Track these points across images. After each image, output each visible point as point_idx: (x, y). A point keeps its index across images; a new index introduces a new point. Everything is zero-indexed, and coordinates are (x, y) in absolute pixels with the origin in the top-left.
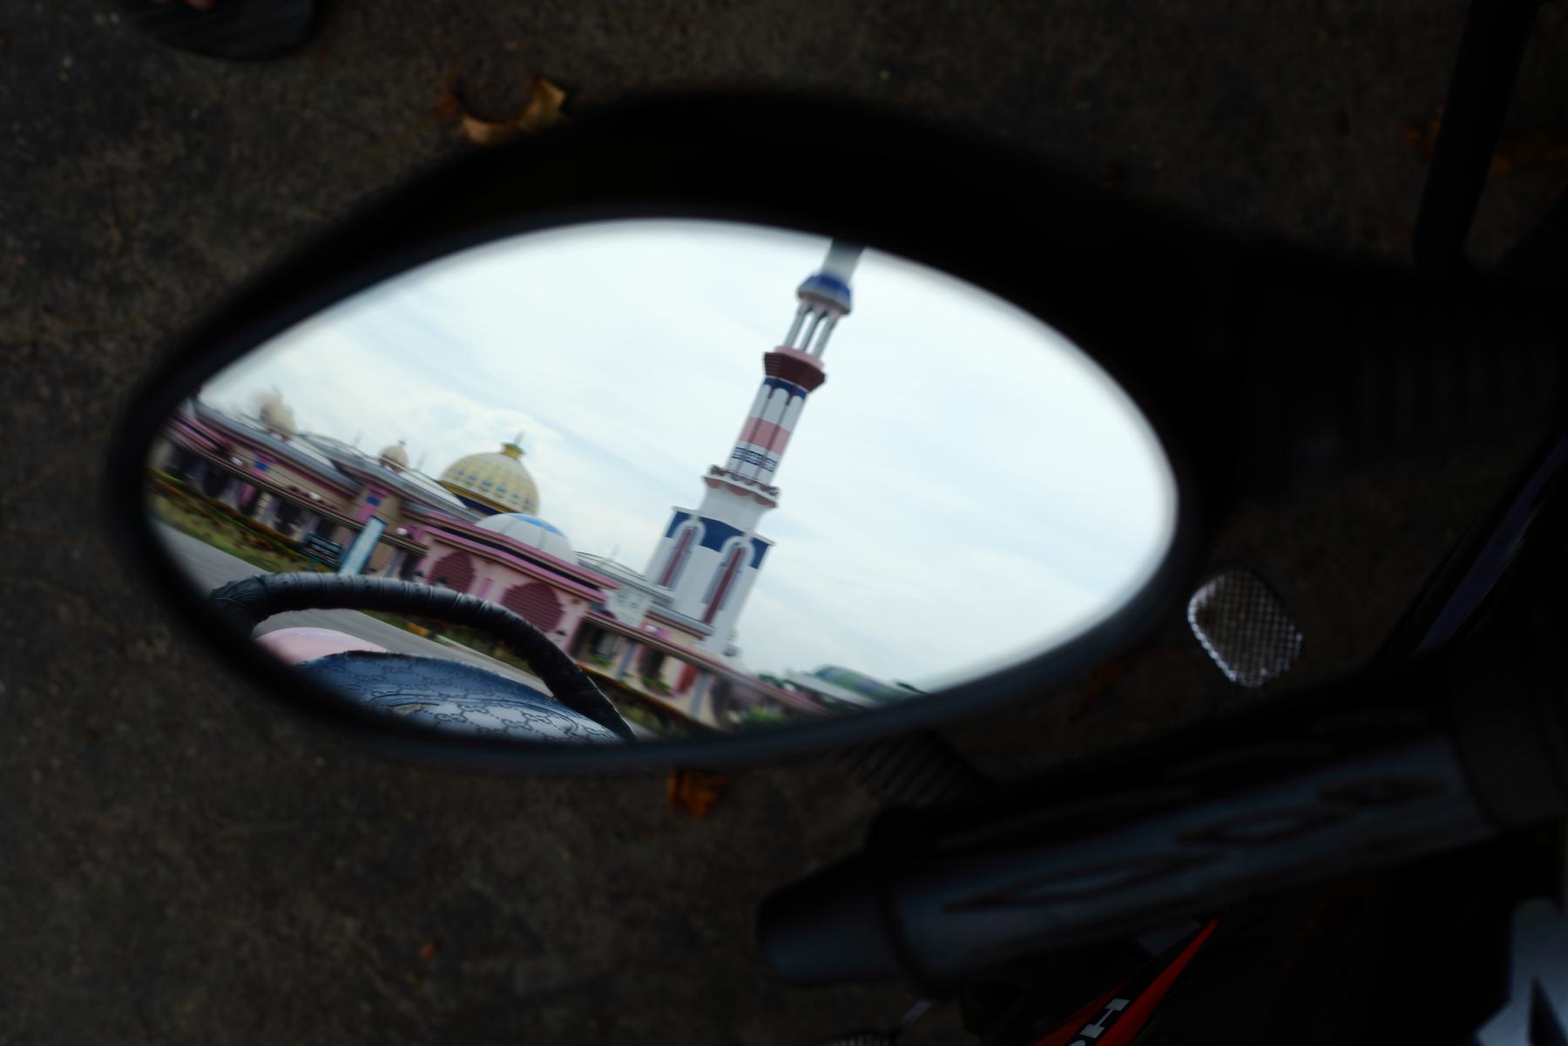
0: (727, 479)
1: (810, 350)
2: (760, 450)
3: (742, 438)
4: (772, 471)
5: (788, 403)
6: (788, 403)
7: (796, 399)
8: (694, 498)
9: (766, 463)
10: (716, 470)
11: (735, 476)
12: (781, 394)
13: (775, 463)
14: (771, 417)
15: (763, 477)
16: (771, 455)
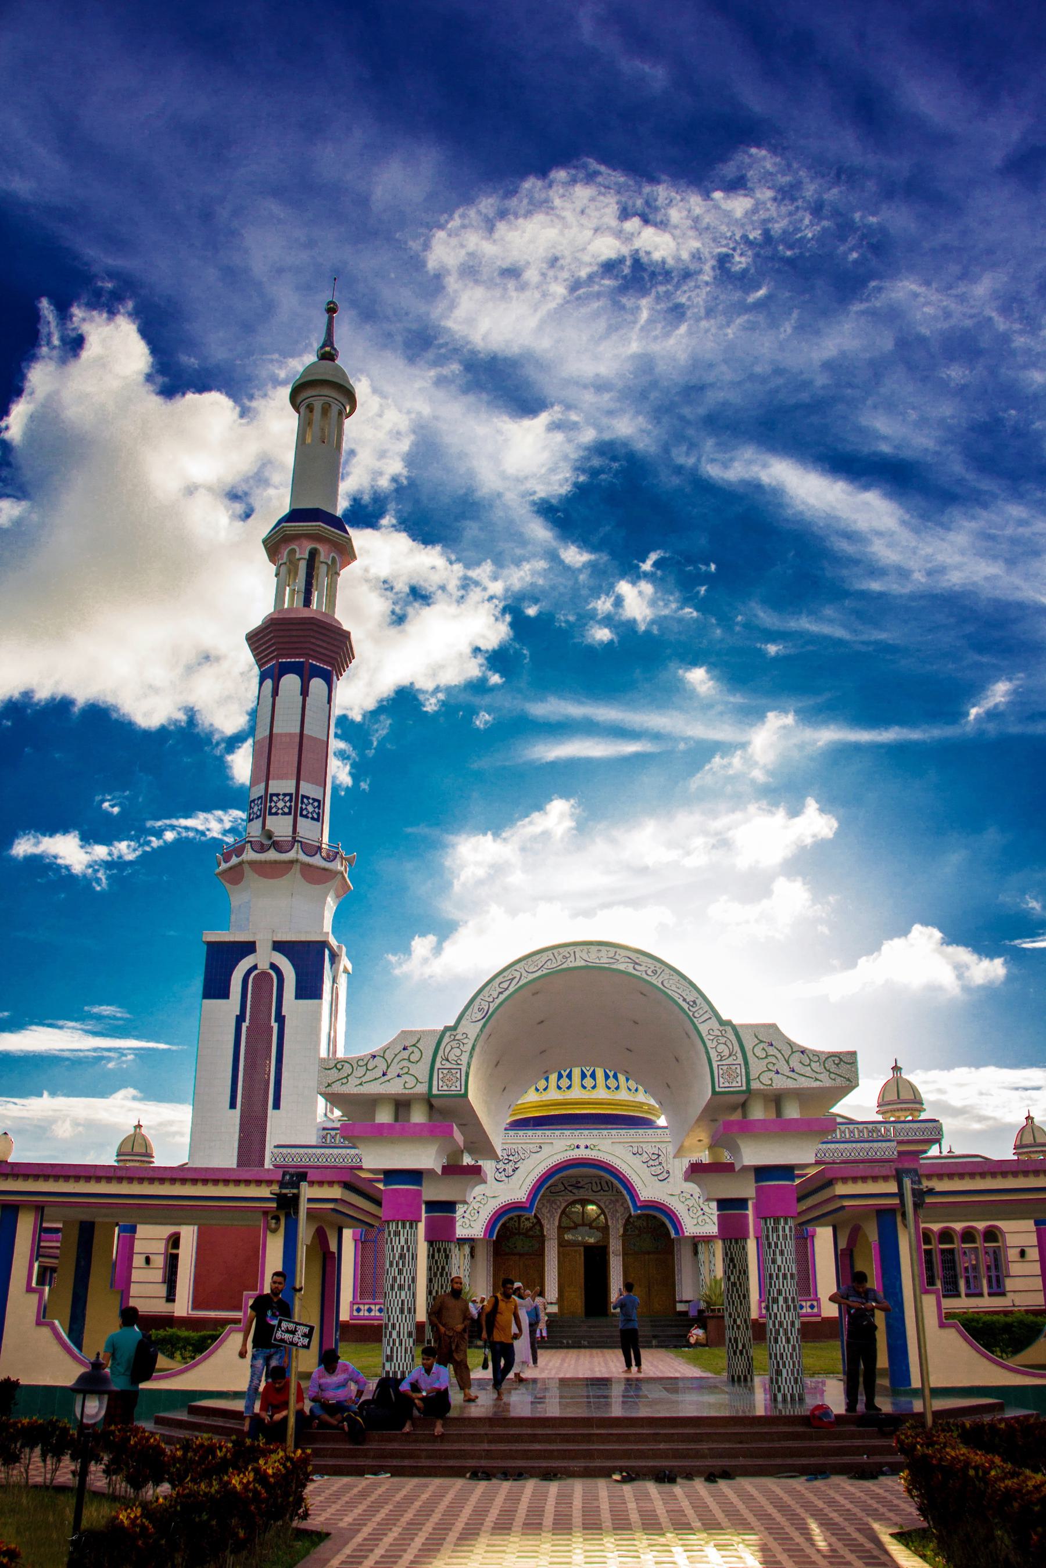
0: (250, 855)
5: (305, 692)
6: (305, 692)
11: (262, 849)
12: (291, 682)
14: (287, 725)
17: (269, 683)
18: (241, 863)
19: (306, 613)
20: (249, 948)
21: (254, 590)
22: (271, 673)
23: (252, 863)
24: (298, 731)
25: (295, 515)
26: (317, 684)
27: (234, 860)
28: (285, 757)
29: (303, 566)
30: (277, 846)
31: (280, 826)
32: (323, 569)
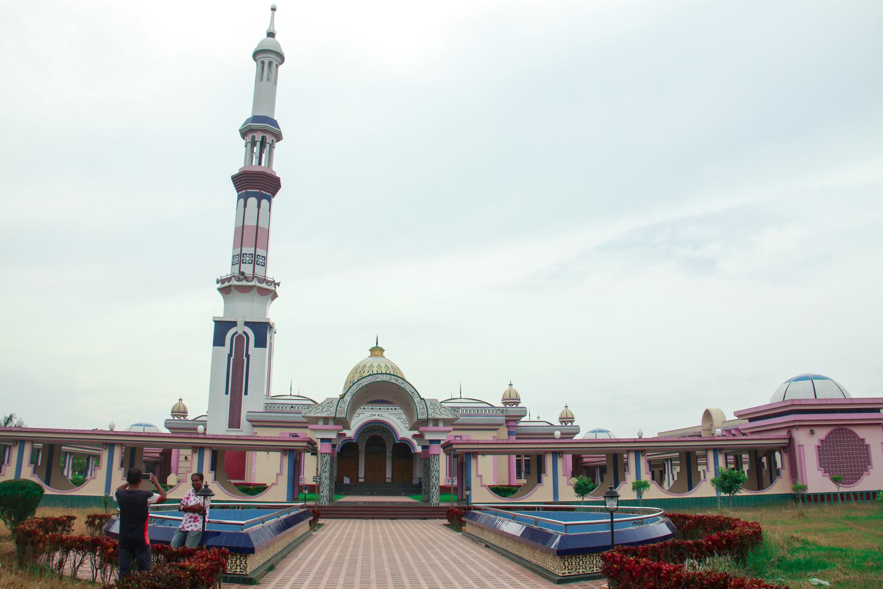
0: (234, 282)
1: (263, 165)
2: (248, 250)
3: (234, 247)
4: (264, 265)
5: (259, 206)
6: (259, 206)
7: (264, 202)
8: (216, 307)
9: (259, 260)
10: (223, 281)
11: (239, 280)
12: (252, 201)
13: (265, 258)
14: (251, 221)
15: (259, 270)
16: (260, 252)
17: (242, 201)
18: (230, 286)
19: (259, 169)
20: (234, 324)
21: (236, 157)
22: (244, 197)
23: (237, 287)
24: (255, 224)
25: (255, 119)
26: (264, 202)
27: (227, 284)
28: (250, 236)
29: (258, 144)
30: (246, 279)
31: (247, 269)
32: (268, 146)
